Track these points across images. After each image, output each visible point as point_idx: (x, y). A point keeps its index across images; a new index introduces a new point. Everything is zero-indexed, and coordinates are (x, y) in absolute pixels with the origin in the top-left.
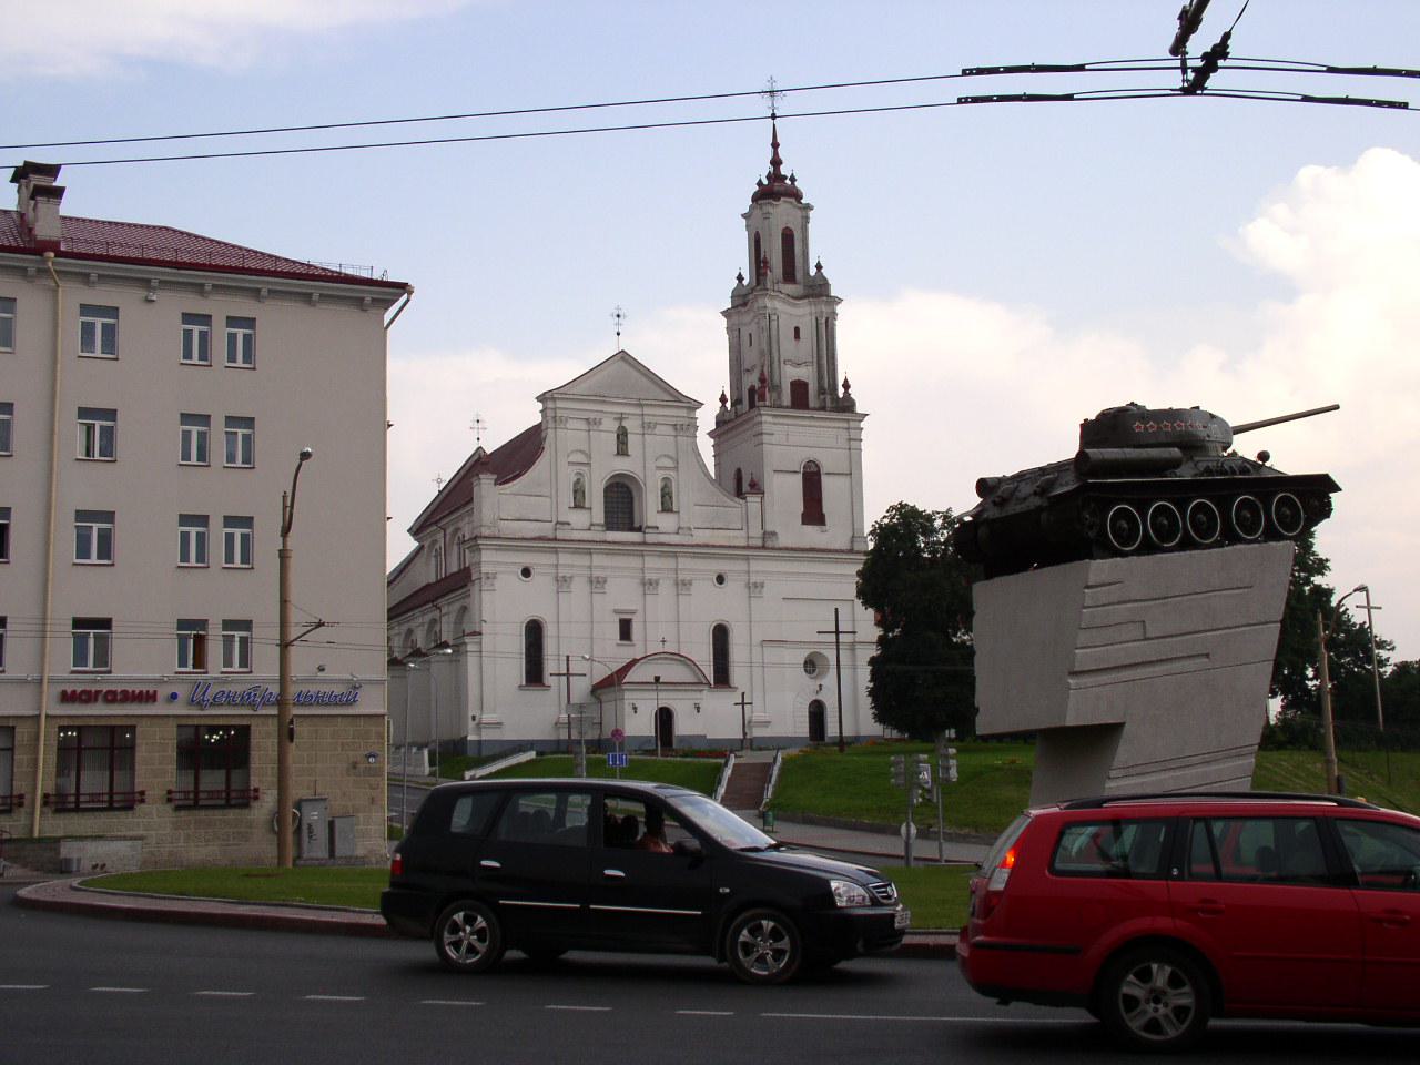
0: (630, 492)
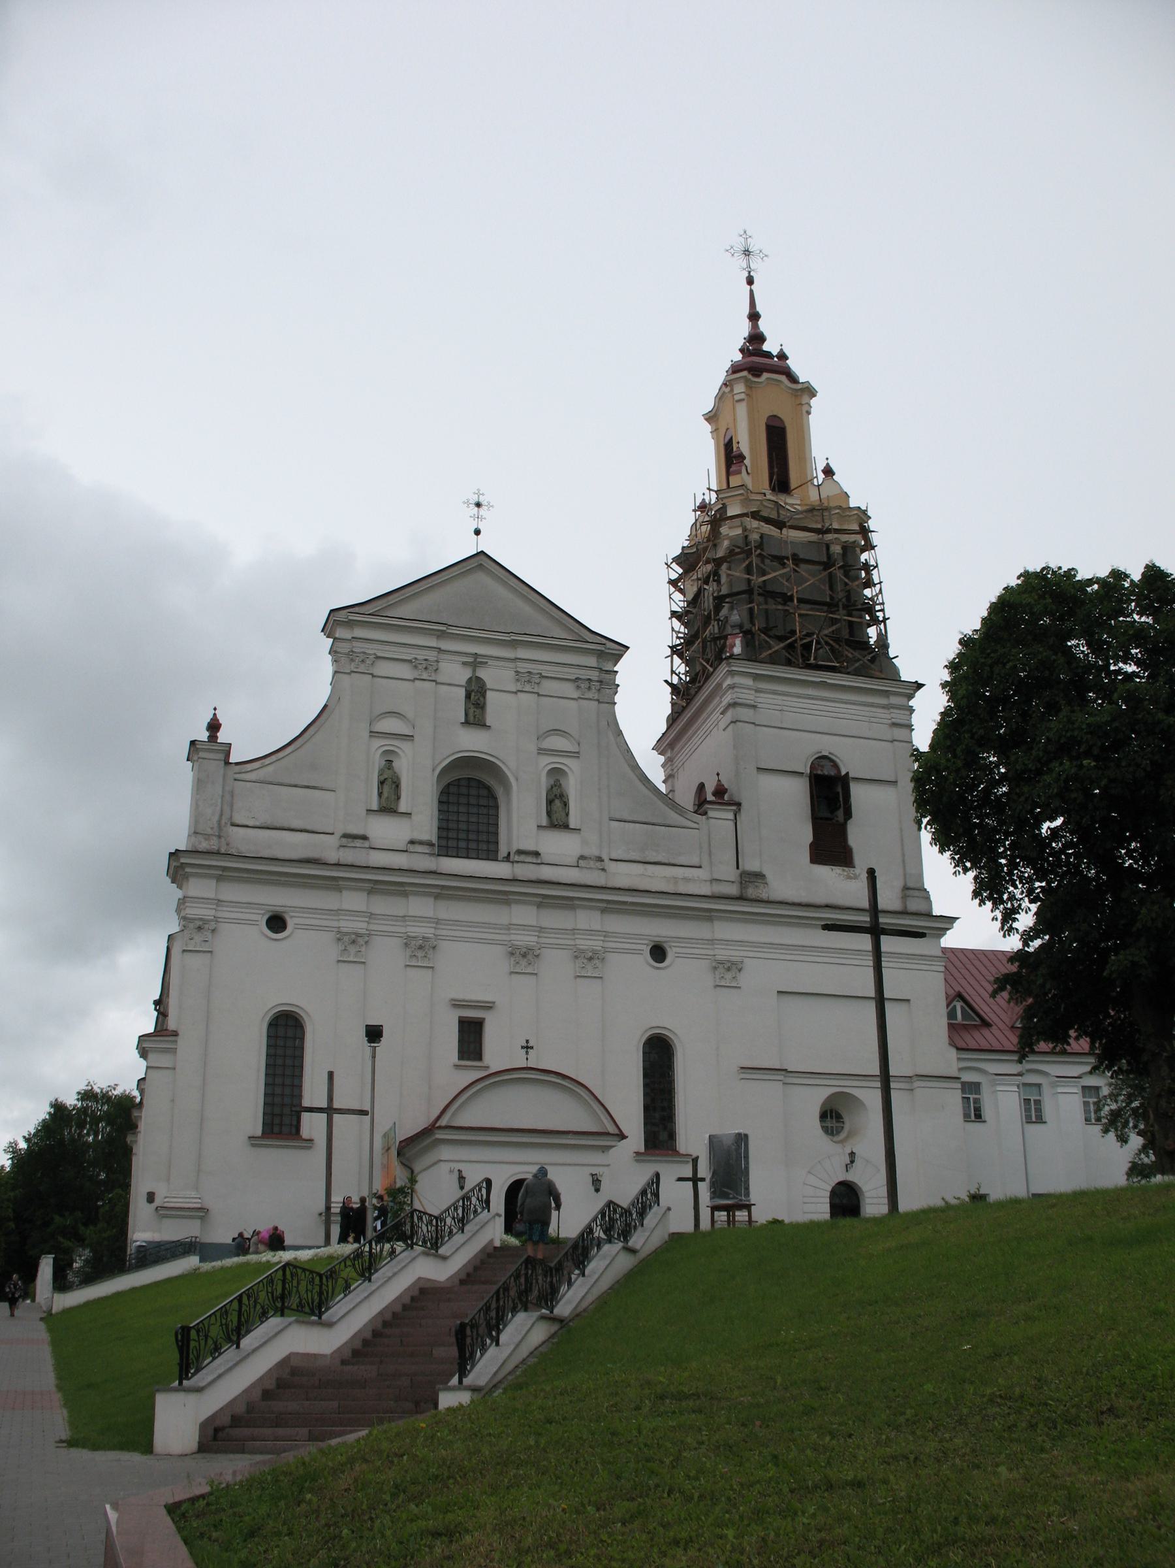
0: (492, 796)
